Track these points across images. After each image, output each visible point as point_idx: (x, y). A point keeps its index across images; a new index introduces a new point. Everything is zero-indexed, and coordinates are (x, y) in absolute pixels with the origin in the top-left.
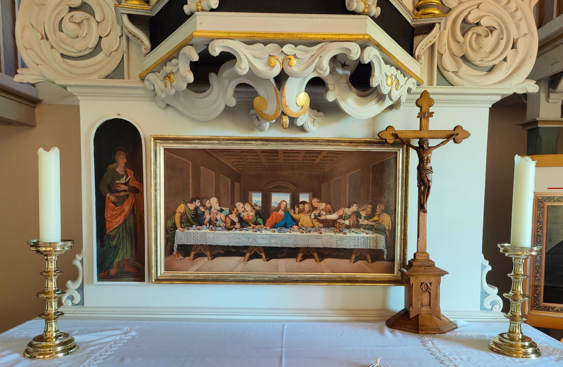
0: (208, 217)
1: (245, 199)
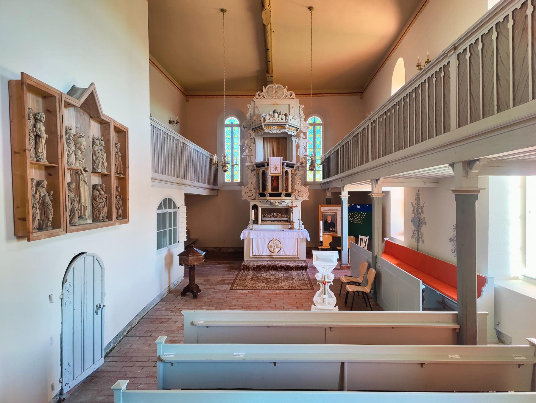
1: (271, 214)
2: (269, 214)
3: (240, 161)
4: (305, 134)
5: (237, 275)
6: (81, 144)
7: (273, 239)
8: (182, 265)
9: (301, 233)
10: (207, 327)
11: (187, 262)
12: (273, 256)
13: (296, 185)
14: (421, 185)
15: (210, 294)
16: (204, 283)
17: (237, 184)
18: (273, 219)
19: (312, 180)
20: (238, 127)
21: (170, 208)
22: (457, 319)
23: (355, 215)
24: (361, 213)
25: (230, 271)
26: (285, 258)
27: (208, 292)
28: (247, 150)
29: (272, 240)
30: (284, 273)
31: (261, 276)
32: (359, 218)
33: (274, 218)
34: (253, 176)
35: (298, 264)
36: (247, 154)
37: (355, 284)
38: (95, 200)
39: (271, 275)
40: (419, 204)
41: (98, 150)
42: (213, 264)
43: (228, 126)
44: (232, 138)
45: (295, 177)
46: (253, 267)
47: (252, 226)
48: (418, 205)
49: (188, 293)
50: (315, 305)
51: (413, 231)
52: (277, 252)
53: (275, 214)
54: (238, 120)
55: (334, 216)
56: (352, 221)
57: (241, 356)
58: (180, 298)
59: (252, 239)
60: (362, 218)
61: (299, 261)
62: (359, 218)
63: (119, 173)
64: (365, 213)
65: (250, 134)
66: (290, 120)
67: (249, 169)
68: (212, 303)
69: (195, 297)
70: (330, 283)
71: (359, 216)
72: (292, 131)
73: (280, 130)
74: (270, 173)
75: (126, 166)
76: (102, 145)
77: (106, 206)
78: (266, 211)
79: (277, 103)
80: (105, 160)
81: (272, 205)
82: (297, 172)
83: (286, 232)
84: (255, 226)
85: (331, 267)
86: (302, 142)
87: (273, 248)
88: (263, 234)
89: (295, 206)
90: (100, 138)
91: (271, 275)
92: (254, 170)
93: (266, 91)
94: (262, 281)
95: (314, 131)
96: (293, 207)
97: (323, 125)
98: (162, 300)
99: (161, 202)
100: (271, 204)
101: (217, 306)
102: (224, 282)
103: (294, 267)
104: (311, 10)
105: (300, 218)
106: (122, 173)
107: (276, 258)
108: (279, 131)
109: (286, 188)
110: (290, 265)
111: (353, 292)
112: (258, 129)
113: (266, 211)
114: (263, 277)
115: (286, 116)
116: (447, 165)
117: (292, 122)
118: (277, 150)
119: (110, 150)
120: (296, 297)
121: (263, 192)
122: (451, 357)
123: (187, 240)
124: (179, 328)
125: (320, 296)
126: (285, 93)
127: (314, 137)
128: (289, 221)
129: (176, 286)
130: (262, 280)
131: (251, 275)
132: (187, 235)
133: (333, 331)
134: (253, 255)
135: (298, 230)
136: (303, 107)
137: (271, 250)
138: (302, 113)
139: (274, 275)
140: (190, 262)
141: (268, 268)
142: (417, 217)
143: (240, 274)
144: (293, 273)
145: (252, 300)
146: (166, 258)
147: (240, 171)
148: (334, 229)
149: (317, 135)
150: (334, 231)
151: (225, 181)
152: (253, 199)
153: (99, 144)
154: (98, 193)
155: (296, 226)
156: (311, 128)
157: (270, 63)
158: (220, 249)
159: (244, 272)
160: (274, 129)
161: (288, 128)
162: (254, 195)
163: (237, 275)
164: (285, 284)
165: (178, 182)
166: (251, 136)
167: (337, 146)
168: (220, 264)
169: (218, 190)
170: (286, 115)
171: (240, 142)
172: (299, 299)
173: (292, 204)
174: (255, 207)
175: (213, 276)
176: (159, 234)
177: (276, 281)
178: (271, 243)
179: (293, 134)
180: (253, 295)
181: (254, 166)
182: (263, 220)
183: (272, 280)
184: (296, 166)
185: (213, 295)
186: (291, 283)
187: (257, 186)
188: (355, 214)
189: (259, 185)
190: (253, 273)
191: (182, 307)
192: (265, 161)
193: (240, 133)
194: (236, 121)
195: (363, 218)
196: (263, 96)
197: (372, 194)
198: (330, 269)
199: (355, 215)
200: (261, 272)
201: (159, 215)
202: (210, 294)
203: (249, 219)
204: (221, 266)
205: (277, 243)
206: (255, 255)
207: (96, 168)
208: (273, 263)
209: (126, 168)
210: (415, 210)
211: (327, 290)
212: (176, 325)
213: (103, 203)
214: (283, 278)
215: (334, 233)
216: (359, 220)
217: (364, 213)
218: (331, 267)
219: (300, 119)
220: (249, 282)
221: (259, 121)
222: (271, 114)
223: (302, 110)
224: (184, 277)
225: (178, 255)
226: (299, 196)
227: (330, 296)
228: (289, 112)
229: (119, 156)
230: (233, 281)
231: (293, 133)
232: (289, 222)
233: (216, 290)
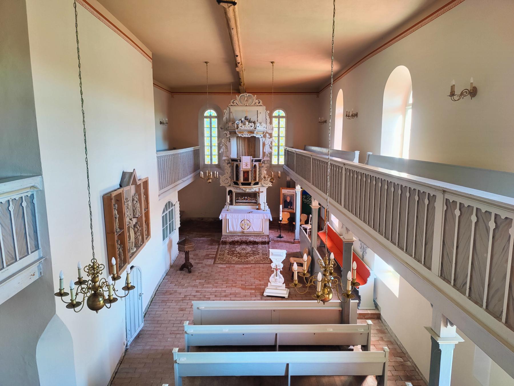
3: (218, 147)
5: (218, 249)
6: (128, 206)
7: (244, 219)
9: (266, 215)
15: (200, 268)
16: (194, 257)
17: (215, 166)
20: (216, 118)
25: (211, 244)
26: (253, 233)
27: (198, 266)
30: (252, 246)
34: (229, 167)
36: (224, 150)
42: (198, 237)
43: (207, 117)
52: (247, 229)
53: (246, 197)
55: (293, 197)
57: (227, 331)
58: (179, 272)
65: (226, 135)
66: (258, 127)
68: (202, 277)
69: (190, 272)
70: (280, 269)
73: (250, 135)
82: (263, 165)
84: (231, 207)
88: (237, 215)
89: (262, 192)
92: (229, 163)
95: (279, 123)
97: (286, 118)
98: (167, 275)
102: (209, 256)
104: (273, 64)
105: (265, 202)
107: (246, 233)
108: (249, 135)
110: (257, 240)
112: (233, 133)
114: (237, 251)
124: (183, 299)
125: (274, 277)
128: (257, 203)
130: (236, 254)
131: (228, 249)
135: (263, 211)
136: (269, 112)
140: (186, 249)
144: (259, 247)
147: (218, 155)
148: (291, 207)
150: (292, 208)
151: (206, 163)
152: (229, 186)
155: (262, 207)
158: (202, 219)
160: (245, 134)
161: (256, 133)
162: (230, 182)
163: (218, 249)
164: (252, 259)
168: (203, 236)
171: (218, 140)
172: (261, 273)
173: (259, 190)
175: (200, 250)
176: (163, 230)
177: (247, 255)
178: (243, 222)
180: (230, 270)
182: (237, 202)
183: (243, 254)
184: (262, 160)
185: (202, 269)
187: (231, 175)
189: (233, 175)
190: (229, 246)
191: (182, 281)
192: (238, 159)
194: (214, 113)
196: (236, 103)
202: (200, 268)
205: (247, 222)
208: (244, 238)
212: (181, 296)
214: (251, 252)
215: (292, 210)
227: (280, 278)
230: (215, 256)
231: (261, 135)
232: (257, 203)
233: (204, 265)
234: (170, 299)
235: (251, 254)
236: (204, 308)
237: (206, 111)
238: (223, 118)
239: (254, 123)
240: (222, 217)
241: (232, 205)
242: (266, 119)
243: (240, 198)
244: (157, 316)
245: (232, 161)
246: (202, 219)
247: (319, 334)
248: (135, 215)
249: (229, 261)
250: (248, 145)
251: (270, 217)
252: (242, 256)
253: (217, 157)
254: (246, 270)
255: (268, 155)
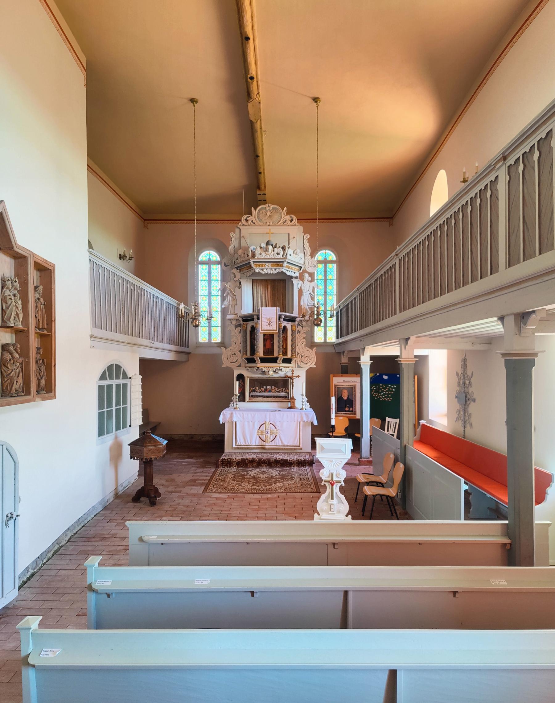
0: (256, 390)
1: (263, 387)
2: (260, 388)
4: (312, 275)
5: (214, 473)
7: (266, 422)
8: (134, 459)
9: (305, 414)
10: (162, 544)
11: (141, 454)
12: (265, 446)
13: (298, 347)
14: (468, 347)
15: (175, 499)
16: (167, 484)
17: (216, 345)
18: (266, 394)
19: (321, 340)
21: (118, 377)
22: (507, 531)
23: (381, 389)
24: (389, 386)
26: (282, 449)
28: (229, 298)
29: (264, 424)
30: (280, 469)
31: (247, 475)
32: (387, 393)
33: (268, 393)
34: (237, 333)
35: (300, 458)
36: (229, 302)
37: (377, 484)
38: (4, 365)
39: (261, 473)
40: (466, 374)
41: (9, 295)
42: (180, 458)
43: (203, 263)
44: (210, 281)
45: (297, 335)
46: (237, 461)
47: (236, 404)
48: (464, 375)
49: (142, 499)
50: (319, 514)
51: (459, 411)
52: (270, 441)
53: (268, 387)
54: (219, 256)
55: (352, 390)
56: (377, 397)
59: (236, 422)
60: (390, 392)
61: (302, 453)
62: (387, 393)
63: (41, 328)
64: (395, 386)
65: (233, 275)
66: (290, 255)
67: (232, 323)
69: (153, 503)
70: (341, 483)
71: (387, 390)
72: (292, 271)
73: (275, 269)
74: (262, 330)
75: (51, 318)
76: (16, 289)
77: (21, 374)
78: (255, 383)
79: (272, 231)
80: (19, 309)
81: (264, 375)
82: (299, 328)
83: (284, 413)
84: (241, 404)
85: (341, 462)
86: (307, 286)
87: (264, 435)
88: (252, 415)
90: (13, 277)
91: (261, 473)
92: (239, 325)
93: (256, 217)
94: (249, 481)
95: (325, 272)
96: (294, 378)
98: (105, 508)
99: (105, 370)
100: (264, 373)
101: (183, 516)
103: (293, 462)
105: (304, 393)
106: (46, 327)
108: (274, 270)
109: (284, 350)
110: (288, 458)
111: (373, 495)
113: (255, 382)
114: (250, 475)
115: (284, 250)
116: (496, 319)
117: (292, 258)
118: (271, 297)
119: (28, 295)
120: (294, 504)
121: (251, 357)
122: (495, 582)
123: (142, 423)
126: (282, 218)
127: (325, 280)
128: (289, 398)
129: (126, 488)
130: (248, 480)
131: (234, 473)
132: (142, 417)
133: (337, 548)
134: (237, 445)
135: (301, 409)
136: (309, 236)
137: (262, 438)
138: (307, 245)
139: (266, 473)
140: (145, 455)
141: (256, 462)
142: (463, 391)
143: (218, 473)
144: (292, 470)
145: (233, 508)
146: (111, 449)
147: (221, 327)
149: (329, 277)
150: (352, 411)
152: (238, 366)
153: (11, 287)
154: (10, 355)
155: (298, 404)
156: (321, 266)
157: (262, 175)
158: (192, 436)
159: (223, 469)
160: (267, 267)
161: (287, 267)
162: (239, 360)
163: (214, 473)
164: (280, 485)
165: (130, 342)
166: (235, 277)
167: (355, 292)
169: (189, 353)
170: (283, 248)
172: (299, 506)
173: (293, 373)
174: (241, 377)
176: (101, 415)
177: (268, 481)
178: (263, 428)
179: (294, 275)
180: (234, 501)
181: (239, 320)
182: (252, 396)
183: (263, 479)
184: (298, 319)
186: (289, 484)
187: (243, 347)
188: (381, 388)
189: (246, 346)
190: (237, 469)
192: (254, 313)
193: (221, 273)
194: (215, 256)
195: (392, 393)
196: (252, 221)
197: (400, 359)
198: (340, 464)
199: (381, 389)
200: (248, 469)
201: (101, 388)
202: (175, 499)
203: (232, 394)
204: (192, 460)
205: (271, 428)
206: (239, 445)
207: (7, 321)
208: (265, 457)
209: (52, 321)
210: (461, 382)
211: (336, 493)
213: (18, 371)
214: (278, 477)
215: (352, 414)
216: (386, 395)
217: (392, 387)
218: (341, 462)
219: (304, 254)
220: (230, 482)
221: (246, 256)
222: (262, 247)
223: (307, 241)
224: (138, 475)
225: (128, 445)
226: (302, 361)
228: (289, 244)
229: (42, 304)
231: (295, 273)
232: (288, 399)
233: (183, 494)
234: (97, 548)
235: (278, 479)
236: (155, 537)
237: (202, 252)
238: (228, 249)
239: (283, 248)
240: (223, 419)
241: (244, 401)
242: (304, 248)
243: (257, 388)
244: (58, 578)
245: (243, 321)
246: (192, 438)
247: (468, 592)
248: (7, 323)
249: (234, 489)
250: (273, 296)
251: (313, 418)
252: (261, 482)
253: (219, 330)
254: (266, 501)
255: (308, 312)
